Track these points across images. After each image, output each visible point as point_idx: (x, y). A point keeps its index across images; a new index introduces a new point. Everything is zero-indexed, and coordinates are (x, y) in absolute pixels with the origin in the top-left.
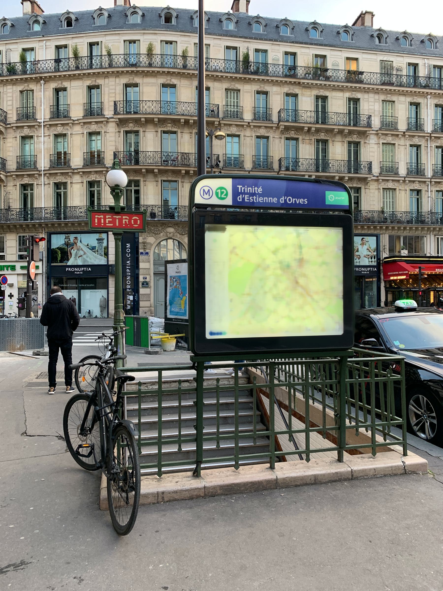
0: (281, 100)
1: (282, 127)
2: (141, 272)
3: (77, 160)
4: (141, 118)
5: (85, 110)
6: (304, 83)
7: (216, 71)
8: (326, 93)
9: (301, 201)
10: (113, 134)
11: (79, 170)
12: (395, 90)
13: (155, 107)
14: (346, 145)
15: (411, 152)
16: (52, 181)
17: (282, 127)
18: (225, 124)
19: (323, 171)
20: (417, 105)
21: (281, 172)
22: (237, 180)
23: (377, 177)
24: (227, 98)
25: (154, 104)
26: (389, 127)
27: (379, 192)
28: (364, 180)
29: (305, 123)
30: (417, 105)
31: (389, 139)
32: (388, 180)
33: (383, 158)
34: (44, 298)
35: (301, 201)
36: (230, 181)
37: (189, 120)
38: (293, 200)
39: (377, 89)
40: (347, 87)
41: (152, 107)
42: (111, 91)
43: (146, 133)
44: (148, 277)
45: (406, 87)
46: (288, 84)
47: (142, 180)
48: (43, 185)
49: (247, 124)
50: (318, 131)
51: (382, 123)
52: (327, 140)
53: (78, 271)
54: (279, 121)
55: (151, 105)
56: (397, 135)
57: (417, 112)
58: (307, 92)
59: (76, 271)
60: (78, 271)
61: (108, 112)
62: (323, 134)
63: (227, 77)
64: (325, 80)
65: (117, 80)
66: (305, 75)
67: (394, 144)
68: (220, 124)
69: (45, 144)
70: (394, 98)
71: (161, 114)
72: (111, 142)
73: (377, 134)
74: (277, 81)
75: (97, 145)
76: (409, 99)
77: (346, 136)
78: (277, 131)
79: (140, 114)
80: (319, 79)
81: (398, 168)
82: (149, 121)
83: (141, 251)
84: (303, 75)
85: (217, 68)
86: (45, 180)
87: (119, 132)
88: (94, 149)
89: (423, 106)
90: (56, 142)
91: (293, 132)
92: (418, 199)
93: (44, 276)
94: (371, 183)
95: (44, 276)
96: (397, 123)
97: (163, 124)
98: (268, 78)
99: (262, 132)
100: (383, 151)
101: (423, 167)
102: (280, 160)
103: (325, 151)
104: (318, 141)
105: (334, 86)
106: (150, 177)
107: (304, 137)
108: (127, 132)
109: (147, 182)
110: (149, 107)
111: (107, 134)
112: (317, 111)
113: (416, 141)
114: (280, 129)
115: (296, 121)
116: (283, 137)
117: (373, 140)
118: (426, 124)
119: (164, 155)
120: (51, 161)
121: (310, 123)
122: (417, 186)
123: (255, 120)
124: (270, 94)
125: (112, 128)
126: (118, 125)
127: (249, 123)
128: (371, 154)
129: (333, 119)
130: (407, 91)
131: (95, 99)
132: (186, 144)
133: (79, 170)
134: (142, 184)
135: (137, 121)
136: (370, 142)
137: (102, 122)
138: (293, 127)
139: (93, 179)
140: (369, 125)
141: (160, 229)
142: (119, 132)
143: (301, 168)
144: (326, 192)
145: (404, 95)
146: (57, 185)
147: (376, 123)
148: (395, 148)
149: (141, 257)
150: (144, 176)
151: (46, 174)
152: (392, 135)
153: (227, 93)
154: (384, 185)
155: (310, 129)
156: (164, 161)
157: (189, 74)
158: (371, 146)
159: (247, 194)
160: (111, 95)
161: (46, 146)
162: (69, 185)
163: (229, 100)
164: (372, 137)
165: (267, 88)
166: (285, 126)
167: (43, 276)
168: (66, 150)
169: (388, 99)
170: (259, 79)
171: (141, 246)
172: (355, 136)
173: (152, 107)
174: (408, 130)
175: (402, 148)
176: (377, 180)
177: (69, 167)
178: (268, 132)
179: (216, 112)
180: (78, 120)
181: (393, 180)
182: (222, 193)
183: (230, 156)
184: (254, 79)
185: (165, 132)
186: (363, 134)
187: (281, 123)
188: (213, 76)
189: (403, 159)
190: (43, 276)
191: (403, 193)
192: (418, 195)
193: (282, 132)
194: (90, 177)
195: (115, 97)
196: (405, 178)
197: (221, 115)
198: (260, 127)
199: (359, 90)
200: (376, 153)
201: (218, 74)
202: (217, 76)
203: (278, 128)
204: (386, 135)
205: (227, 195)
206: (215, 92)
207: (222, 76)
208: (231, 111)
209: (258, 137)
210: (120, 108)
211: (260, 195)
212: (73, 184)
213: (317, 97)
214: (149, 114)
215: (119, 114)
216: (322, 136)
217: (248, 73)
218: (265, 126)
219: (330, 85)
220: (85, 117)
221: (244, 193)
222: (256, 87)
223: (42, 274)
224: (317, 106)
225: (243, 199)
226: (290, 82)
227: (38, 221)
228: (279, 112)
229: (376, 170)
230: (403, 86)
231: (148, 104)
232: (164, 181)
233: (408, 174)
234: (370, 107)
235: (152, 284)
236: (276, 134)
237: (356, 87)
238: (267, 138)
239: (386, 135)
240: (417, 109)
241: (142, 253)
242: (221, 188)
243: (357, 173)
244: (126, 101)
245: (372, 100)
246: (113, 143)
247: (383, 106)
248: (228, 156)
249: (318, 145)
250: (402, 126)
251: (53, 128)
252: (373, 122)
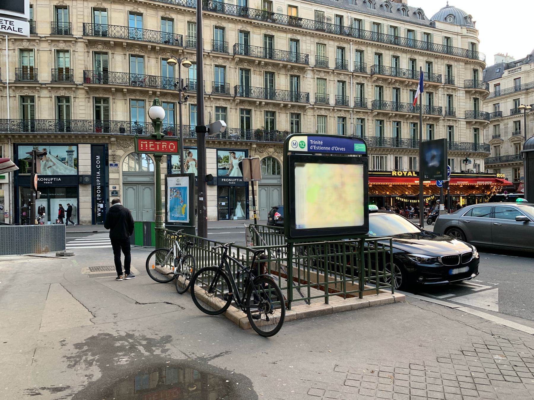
0: (236, 36)
1: (237, 59)
2: (111, 182)
3: (45, 75)
4: (110, 41)
5: (53, 29)
6: (254, 23)
7: (178, 4)
8: (273, 33)
9: (342, 149)
10: (82, 54)
11: (47, 86)
12: (326, 36)
13: (124, 32)
14: (289, 78)
15: (339, 86)
16: (18, 94)
17: (237, 59)
18: (187, 53)
19: (271, 99)
20: (343, 49)
21: (237, 98)
23: (313, 105)
24: (189, 29)
25: (123, 30)
26: (322, 64)
27: (315, 118)
28: (303, 108)
29: (256, 57)
30: (343, 49)
31: (322, 75)
32: (321, 109)
33: (317, 90)
34: (11, 207)
35: (342, 149)
37: (155, 46)
39: (313, 33)
40: (289, 29)
41: (121, 32)
42: (79, 13)
43: (115, 55)
44: (117, 186)
45: (334, 34)
46: (241, 23)
47: (111, 97)
48: (8, 97)
49: (207, 54)
50: (266, 64)
51: (317, 61)
52: (274, 73)
53: (47, 181)
54: (235, 54)
55: (119, 29)
56: (328, 72)
57: (342, 54)
58: (257, 31)
59: (46, 181)
60: (47, 181)
61: (77, 32)
62: (270, 67)
63: (189, 11)
64: (272, 22)
65: (85, 3)
66: (256, 15)
67: (326, 79)
68: (183, 52)
69: (10, 57)
70: (326, 42)
71: (128, 39)
72: (80, 61)
73: (313, 70)
74: (232, 19)
75: (65, 62)
76: (337, 44)
77: (288, 70)
78: (232, 62)
79: (109, 37)
80: (267, 21)
81: (329, 99)
82: (118, 45)
83: (110, 162)
84: (254, 16)
85: (181, 2)
86: (11, 93)
87: (88, 52)
88: (62, 66)
89: (347, 50)
90: (21, 57)
91: (246, 64)
92: (343, 124)
93: (11, 185)
94: (308, 110)
95: (11, 185)
96: (328, 62)
97: (131, 48)
98: (225, 16)
99: (220, 62)
100: (317, 85)
101: (347, 99)
102: (236, 87)
103: (272, 81)
104: (266, 73)
105: (279, 27)
106: (119, 95)
107: (255, 69)
108: (96, 53)
109: (116, 100)
110: (118, 32)
111: (76, 53)
112: (266, 48)
113: (342, 78)
114: (236, 61)
115: (246, 54)
116: (237, 67)
117: (309, 74)
118: (349, 65)
119: (133, 77)
120: (16, 74)
121: (260, 57)
122: (343, 114)
123: (214, 51)
124: (227, 30)
125: (80, 47)
126: (87, 45)
127: (209, 53)
128: (308, 86)
129: (278, 55)
130: (335, 37)
131: (62, 19)
132: (153, 68)
133: (47, 86)
134: (111, 101)
135: (106, 44)
136: (308, 76)
137: (71, 41)
138: (246, 59)
139: (62, 94)
140: (307, 62)
141: (129, 142)
142: (88, 52)
143: (253, 95)
145: (333, 40)
146: (23, 98)
147: (312, 61)
148: (326, 82)
149: (111, 169)
150: (113, 94)
151: (11, 86)
152: (324, 72)
153: (189, 26)
154: (317, 113)
155: (260, 62)
156: (133, 82)
157: (155, 5)
158: (309, 79)
160: (79, 17)
161: (10, 59)
162: (36, 99)
163: (191, 31)
164: (309, 72)
165: (224, 24)
166: (239, 58)
167: (9, 186)
168: (32, 65)
169: (321, 42)
170: (217, 16)
171: (110, 158)
172: (296, 71)
173: (121, 32)
174: (336, 68)
175: (332, 83)
176: (313, 108)
177: (36, 81)
178: (225, 62)
179: (180, 42)
180: (45, 37)
181: (325, 109)
182: (302, 144)
183: (192, 81)
184: (213, 15)
185: (132, 56)
186: (302, 70)
187: (236, 56)
188: (176, 9)
189: (332, 92)
190: (9, 186)
191: (332, 119)
192: (343, 121)
193: (237, 64)
194: (59, 93)
195: (83, 19)
196: (334, 107)
197: (184, 44)
198: (218, 57)
199: (299, 33)
200: (312, 86)
201: (181, 8)
202: (181, 10)
203: (233, 59)
204: (320, 71)
205: (305, 145)
206: (179, 23)
207: (185, 10)
208: (192, 41)
209: (216, 66)
210: (89, 29)
212: (41, 99)
213: (266, 36)
214: (118, 38)
215: (88, 35)
216: (270, 69)
217: (208, 10)
218: (222, 57)
219: (276, 27)
220: (52, 35)
222: (214, 23)
223: (9, 184)
224: (266, 43)
225: (313, 148)
226: (244, 21)
227: (3, 132)
228: (234, 46)
229: (312, 100)
230: (332, 33)
231: (117, 29)
232: (132, 100)
233: (336, 104)
234: (308, 48)
235: (121, 193)
236: (232, 64)
237: (296, 30)
238: (224, 67)
239: (320, 71)
240: (342, 52)
241: (111, 165)
242: (302, 142)
243: (297, 102)
244: (94, 24)
245: (308, 42)
246: (83, 62)
247: (317, 48)
248: (190, 80)
249: (266, 76)
250: (332, 65)
251: (18, 43)
252: (310, 60)
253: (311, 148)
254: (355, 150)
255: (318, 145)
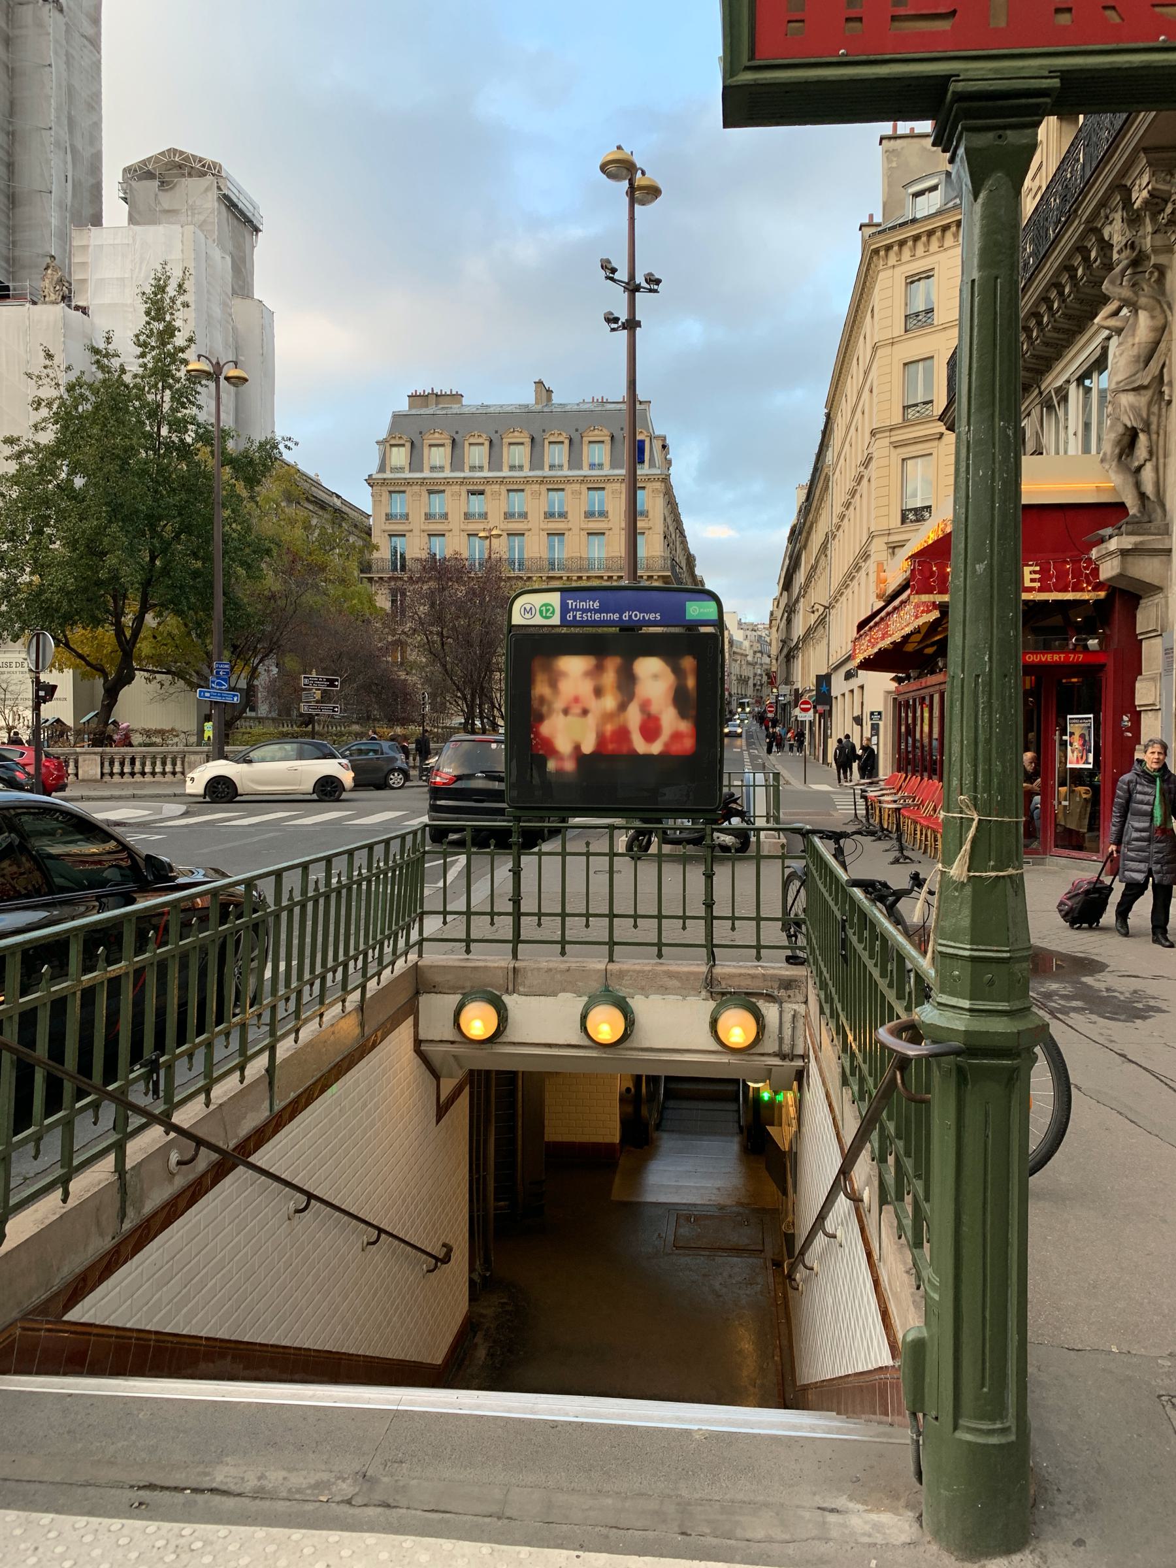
22: (566, 594)
36: (557, 595)
38: (640, 616)
144: (688, 604)
159: (579, 610)
182: (547, 611)
205: (553, 613)
211: (596, 611)
221: (577, 610)
225: (575, 617)
242: (546, 605)
253: (570, 617)
254: (688, 618)
255: (588, 609)
